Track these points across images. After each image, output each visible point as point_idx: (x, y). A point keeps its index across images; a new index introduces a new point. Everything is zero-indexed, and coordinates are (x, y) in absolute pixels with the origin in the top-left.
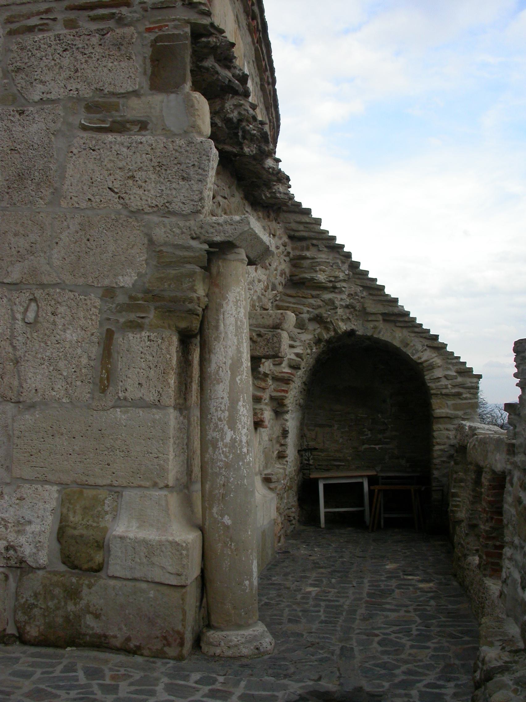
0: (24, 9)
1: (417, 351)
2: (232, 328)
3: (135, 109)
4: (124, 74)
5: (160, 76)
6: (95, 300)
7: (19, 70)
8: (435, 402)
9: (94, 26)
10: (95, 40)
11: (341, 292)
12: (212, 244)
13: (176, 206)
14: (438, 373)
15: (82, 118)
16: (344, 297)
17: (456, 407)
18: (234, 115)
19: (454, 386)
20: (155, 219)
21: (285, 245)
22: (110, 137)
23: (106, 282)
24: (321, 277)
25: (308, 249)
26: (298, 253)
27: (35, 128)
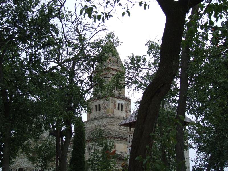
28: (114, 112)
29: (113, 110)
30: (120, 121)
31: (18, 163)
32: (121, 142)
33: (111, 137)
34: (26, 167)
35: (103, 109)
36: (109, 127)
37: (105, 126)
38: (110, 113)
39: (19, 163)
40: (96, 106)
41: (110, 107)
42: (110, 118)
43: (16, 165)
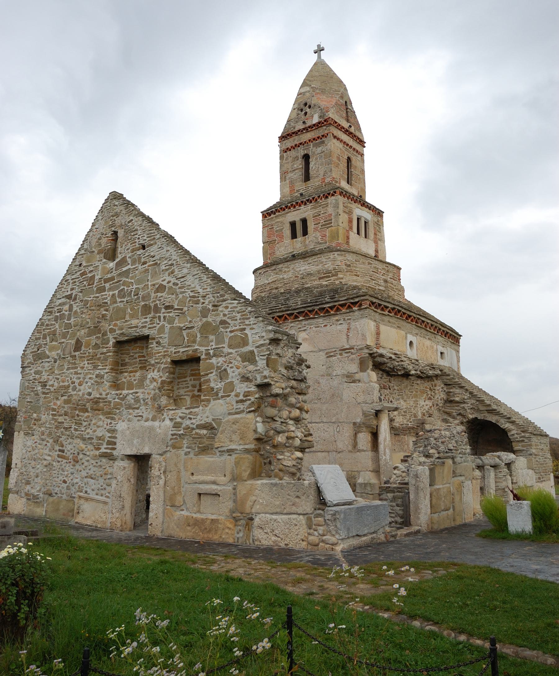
0: (330, 350)
1: (503, 424)
2: (383, 431)
3: (357, 376)
4: (354, 368)
5: (363, 367)
6: (352, 425)
7: (330, 367)
8: (513, 444)
9: (346, 355)
10: (346, 359)
11: (468, 403)
12: (376, 411)
13: (368, 401)
14: (513, 432)
15: (345, 379)
16: (469, 405)
17: (523, 446)
18: (392, 366)
19: (521, 437)
20: (363, 405)
21: (442, 388)
22: (352, 384)
23: (354, 421)
24: (457, 399)
25: (452, 388)
26: (448, 390)
27: (335, 383)
28: (350, 237)
29: (348, 231)
30: (369, 263)
31: (61, 384)
32: (391, 320)
33: (368, 303)
34: (92, 396)
35: (316, 230)
36: (342, 278)
37: (329, 277)
38: (340, 239)
39: (66, 384)
40: (293, 225)
41: (341, 224)
42: (343, 253)
43: (56, 391)
